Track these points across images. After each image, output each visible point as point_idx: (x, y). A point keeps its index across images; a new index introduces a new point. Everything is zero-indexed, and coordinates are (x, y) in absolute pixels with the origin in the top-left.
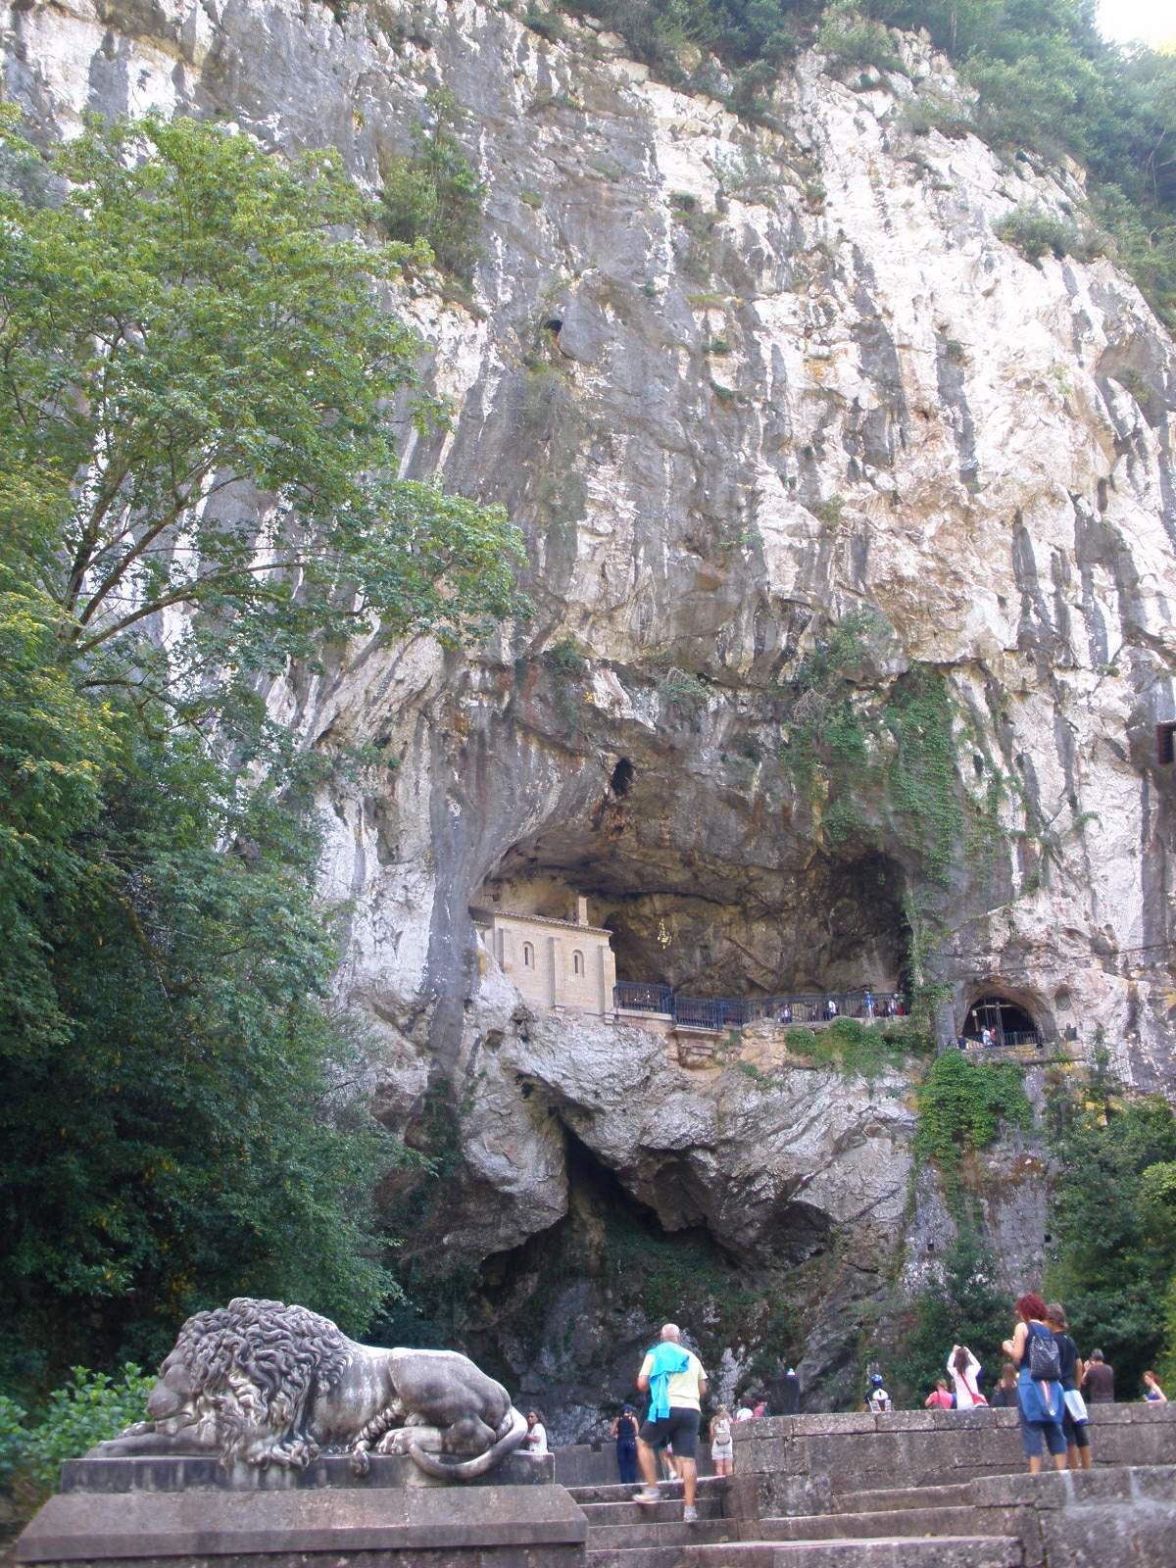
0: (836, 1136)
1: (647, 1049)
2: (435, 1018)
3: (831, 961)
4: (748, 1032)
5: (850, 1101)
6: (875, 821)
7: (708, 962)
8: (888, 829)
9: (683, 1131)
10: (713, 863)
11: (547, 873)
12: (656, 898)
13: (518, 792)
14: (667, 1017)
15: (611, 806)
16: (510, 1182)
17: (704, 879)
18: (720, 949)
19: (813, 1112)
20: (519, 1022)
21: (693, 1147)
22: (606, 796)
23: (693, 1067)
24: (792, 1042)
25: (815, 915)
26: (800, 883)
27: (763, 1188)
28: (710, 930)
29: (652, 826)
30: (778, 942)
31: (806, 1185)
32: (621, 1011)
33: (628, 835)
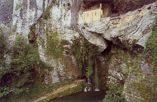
0: (142, 31)
1: (106, 23)
2: (75, 27)
5: (146, 23)
9: (115, 34)
14: (110, 17)
16: (97, 44)
19: (138, 27)
21: (117, 37)
27: (130, 42)
31: (138, 41)
32: (101, 19)
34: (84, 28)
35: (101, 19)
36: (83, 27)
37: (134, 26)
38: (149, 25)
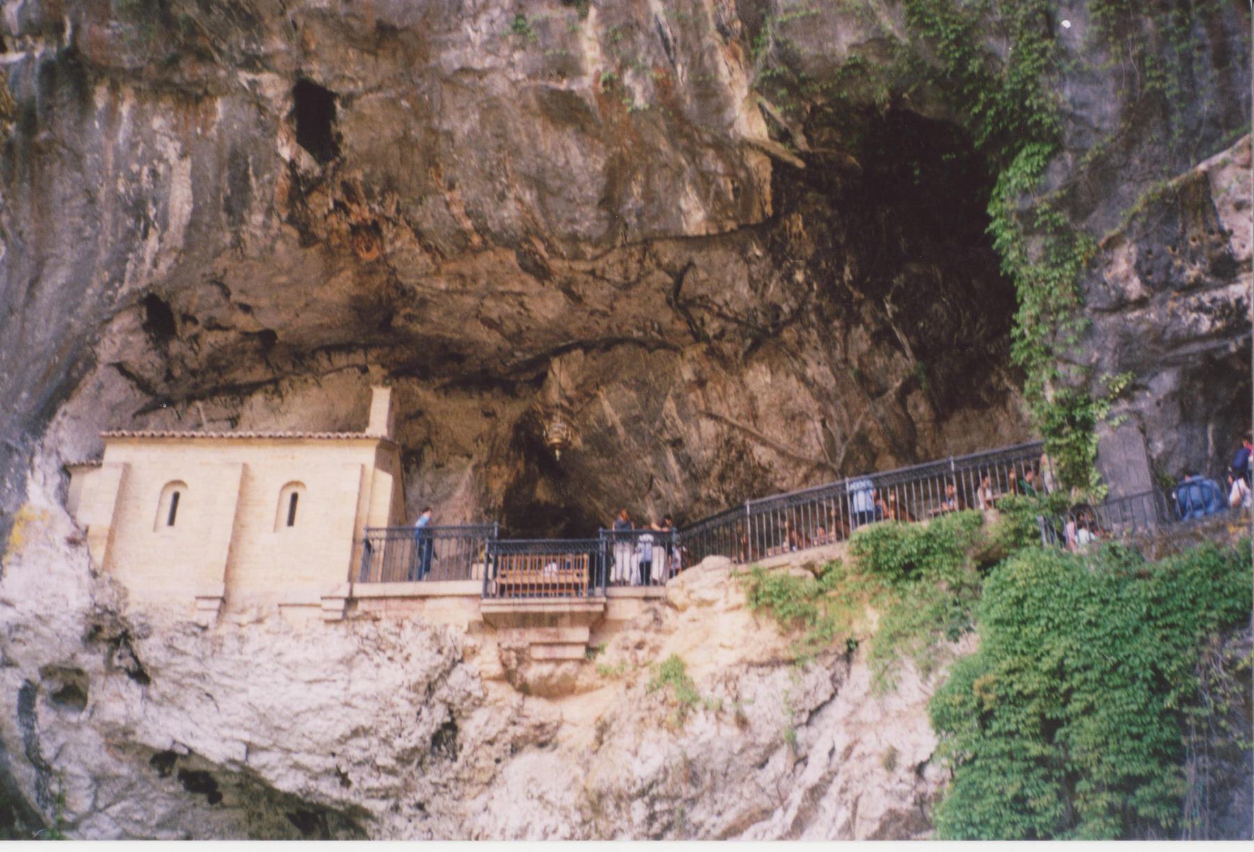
1: (423, 661)
3: (940, 418)
4: (677, 596)
6: (844, 41)
7: (695, 476)
8: (884, 44)
10: (577, 256)
11: (340, 360)
12: (556, 364)
13: (102, 194)
15: (314, 185)
17: (596, 295)
18: (703, 436)
19: (811, 775)
20: (115, 642)
22: (292, 165)
23: (554, 691)
24: (762, 600)
25: (852, 320)
26: (778, 252)
28: (670, 406)
29: (445, 210)
30: (803, 399)
32: (360, 590)
33: (400, 243)
34: (71, 691)
35: (360, 590)
36: (47, 672)
37: (772, 748)
38: (930, 772)
